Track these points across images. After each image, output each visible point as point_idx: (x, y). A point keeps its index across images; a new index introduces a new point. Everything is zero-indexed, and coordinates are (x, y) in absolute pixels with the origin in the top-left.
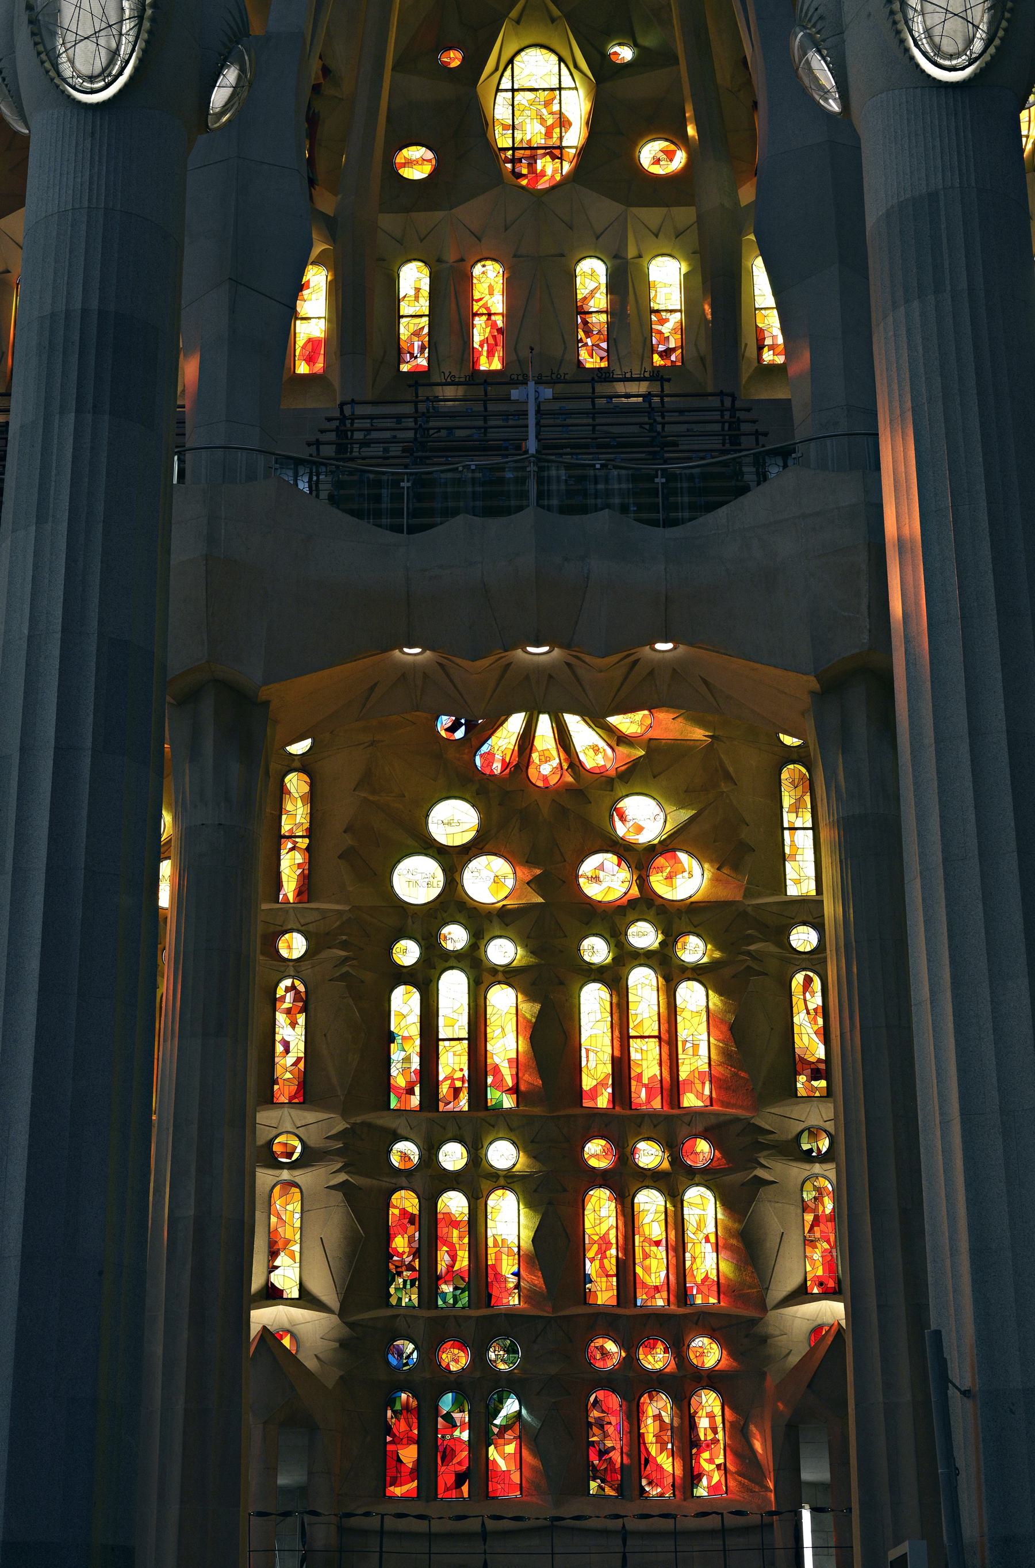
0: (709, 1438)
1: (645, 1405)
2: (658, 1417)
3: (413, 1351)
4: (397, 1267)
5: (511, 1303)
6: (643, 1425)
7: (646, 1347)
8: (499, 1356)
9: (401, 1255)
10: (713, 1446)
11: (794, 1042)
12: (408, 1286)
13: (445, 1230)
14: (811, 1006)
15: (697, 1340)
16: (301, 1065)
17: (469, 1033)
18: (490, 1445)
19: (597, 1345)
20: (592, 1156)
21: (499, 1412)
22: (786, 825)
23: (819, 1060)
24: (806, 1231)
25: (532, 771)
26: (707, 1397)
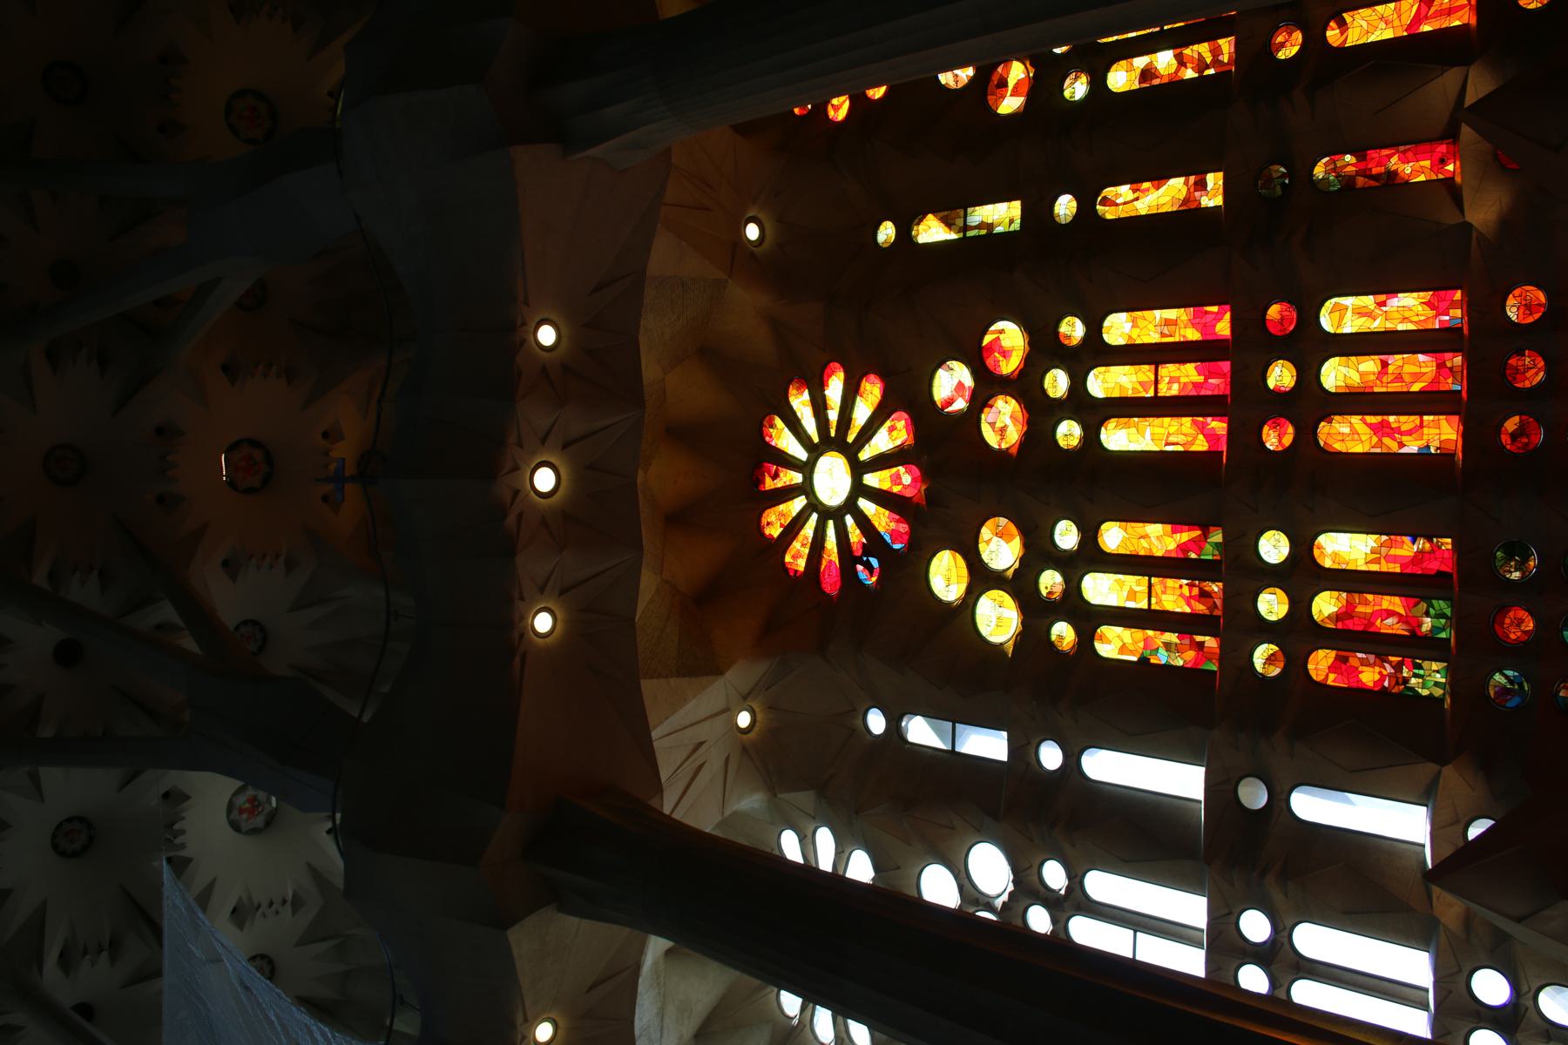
4: (1397, 683)
5: (1450, 547)
7: (1515, 379)
9: (1383, 677)
11: (1166, 213)
12: (1421, 672)
14: (1131, 196)
15: (1509, 314)
17: (1143, 575)
23: (1186, 183)
24: (1377, 184)
25: (908, 494)
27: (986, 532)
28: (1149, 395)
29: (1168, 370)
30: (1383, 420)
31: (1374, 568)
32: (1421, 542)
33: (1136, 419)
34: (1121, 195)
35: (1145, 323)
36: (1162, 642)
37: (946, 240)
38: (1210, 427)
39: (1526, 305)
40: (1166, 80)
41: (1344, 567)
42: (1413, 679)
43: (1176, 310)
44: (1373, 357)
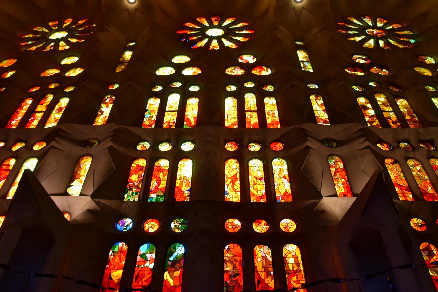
0: (295, 269)
1: (257, 251)
2: (264, 258)
3: (131, 223)
6: (256, 262)
7: (256, 223)
9: (132, 182)
12: (134, 195)
13: (157, 173)
16: (107, 118)
18: (166, 271)
19: (230, 221)
21: (173, 253)
22: (300, 60)
23: (326, 118)
26: (292, 247)
27: (195, 69)
28: (246, 109)
29: (255, 115)
30: (238, 179)
31: (178, 178)
33: (237, 106)
36: (153, 115)
37: (298, 57)
39: (288, 226)
40: (363, 112)
41: (179, 168)
42: (132, 192)
43: (278, 116)
44: (263, 175)
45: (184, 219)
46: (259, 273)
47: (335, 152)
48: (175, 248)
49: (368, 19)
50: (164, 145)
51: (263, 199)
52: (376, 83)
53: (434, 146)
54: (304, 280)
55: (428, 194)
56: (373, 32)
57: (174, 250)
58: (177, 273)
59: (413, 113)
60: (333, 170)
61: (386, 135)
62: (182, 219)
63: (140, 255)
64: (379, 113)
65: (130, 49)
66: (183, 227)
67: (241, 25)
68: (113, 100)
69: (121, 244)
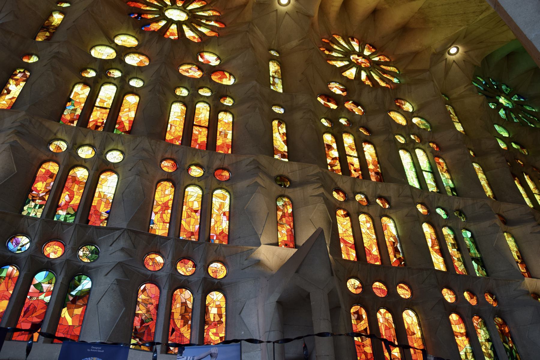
0: (216, 320)
2: (184, 304)
3: (27, 243)
6: (173, 308)
7: (182, 263)
8: (85, 254)
9: (36, 190)
10: (218, 325)
11: (273, 143)
12: (37, 208)
14: (281, 132)
16: (14, 100)
17: (111, 107)
20: (165, 166)
22: (271, 75)
23: (285, 152)
27: (142, 58)
28: (194, 122)
29: (205, 132)
31: (96, 195)
32: (106, 216)
33: (184, 116)
34: (282, 129)
35: (227, 127)
38: (177, 141)
40: (327, 152)
41: (99, 183)
42: (34, 204)
43: (231, 138)
45: (95, 247)
46: (175, 320)
47: (286, 194)
48: (80, 280)
49: (356, 42)
50: (85, 150)
51: (194, 235)
52: (348, 121)
53: (389, 204)
54: (224, 333)
55: (371, 255)
56: (358, 59)
57: (78, 283)
58: (78, 311)
59: (377, 163)
60: (280, 213)
61: (344, 183)
62: (94, 247)
63: (34, 285)
64: (343, 157)
65: (62, 11)
66: (93, 257)
67: (210, 13)
68: (26, 77)
69: (10, 269)
